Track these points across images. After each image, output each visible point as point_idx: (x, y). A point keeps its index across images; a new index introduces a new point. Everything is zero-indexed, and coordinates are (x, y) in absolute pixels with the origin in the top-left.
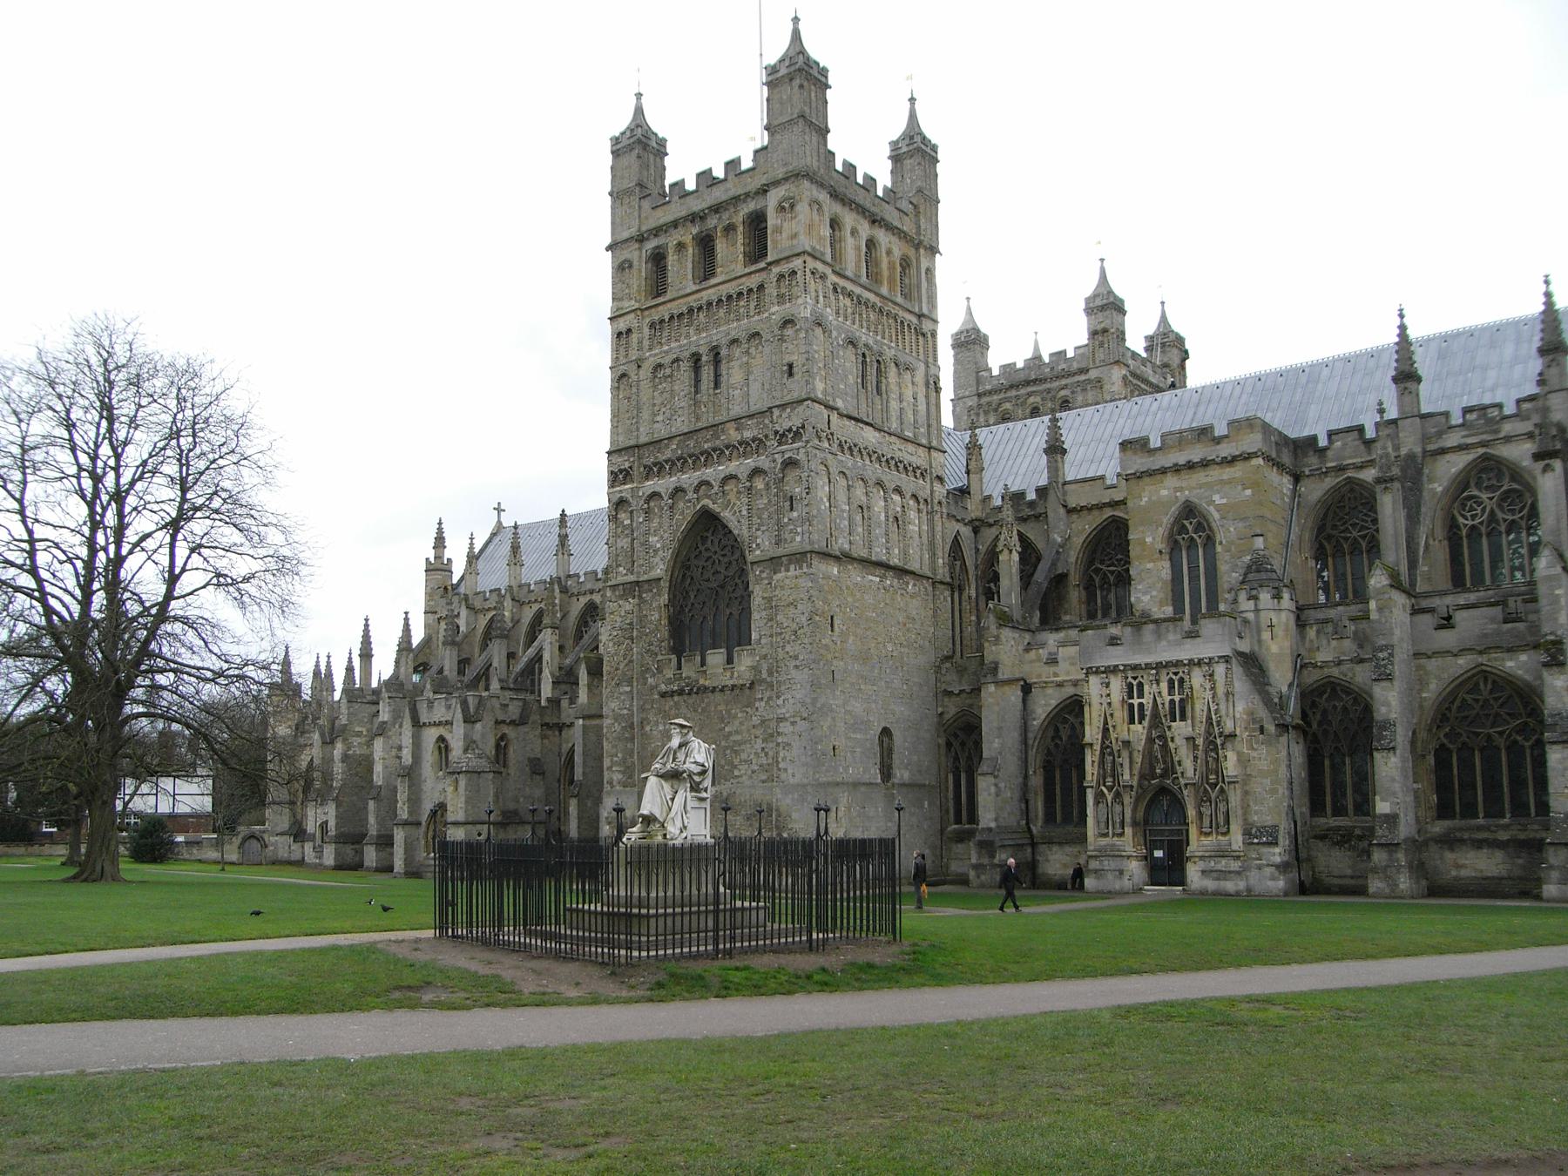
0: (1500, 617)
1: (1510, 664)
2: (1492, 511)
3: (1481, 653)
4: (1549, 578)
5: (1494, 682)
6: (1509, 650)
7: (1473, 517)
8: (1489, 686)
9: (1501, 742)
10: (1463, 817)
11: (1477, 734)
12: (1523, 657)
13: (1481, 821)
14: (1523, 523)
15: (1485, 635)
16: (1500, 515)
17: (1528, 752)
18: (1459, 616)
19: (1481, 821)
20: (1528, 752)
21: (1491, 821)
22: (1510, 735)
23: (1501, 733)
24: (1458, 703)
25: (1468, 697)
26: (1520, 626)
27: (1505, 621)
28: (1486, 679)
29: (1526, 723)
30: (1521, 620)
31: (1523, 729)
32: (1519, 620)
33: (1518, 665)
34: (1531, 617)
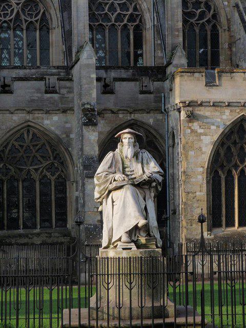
0: (43, 89)
1: (46, 122)
2: (18, 13)
3: (29, 112)
4: (88, 66)
5: (34, 134)
6: (47, 112)
7: (5, 15)
8: (30, 137)
9: (36, 176)
10: (9, 228)
11: (21, 170)
12: (55, 118)
13: (21, 231)
14: (38, 25)
15: (33, 101)
16: (23, 17)
17: (53, 183)
18: (17, 85)
19: (38, 231)
20: (53, 183)
21: (28, 231)
22: (42, 172)
23: (36, 170)
24: (9, 148)
25: (16, 144)
26: (56, 96)
27: (46, 92)
28: (28, 131)
29: (53, 164)
30: (56, 93)
31: (50, 168)
32: (54, 92)
33: (52, 123)
34: (64, 91)
